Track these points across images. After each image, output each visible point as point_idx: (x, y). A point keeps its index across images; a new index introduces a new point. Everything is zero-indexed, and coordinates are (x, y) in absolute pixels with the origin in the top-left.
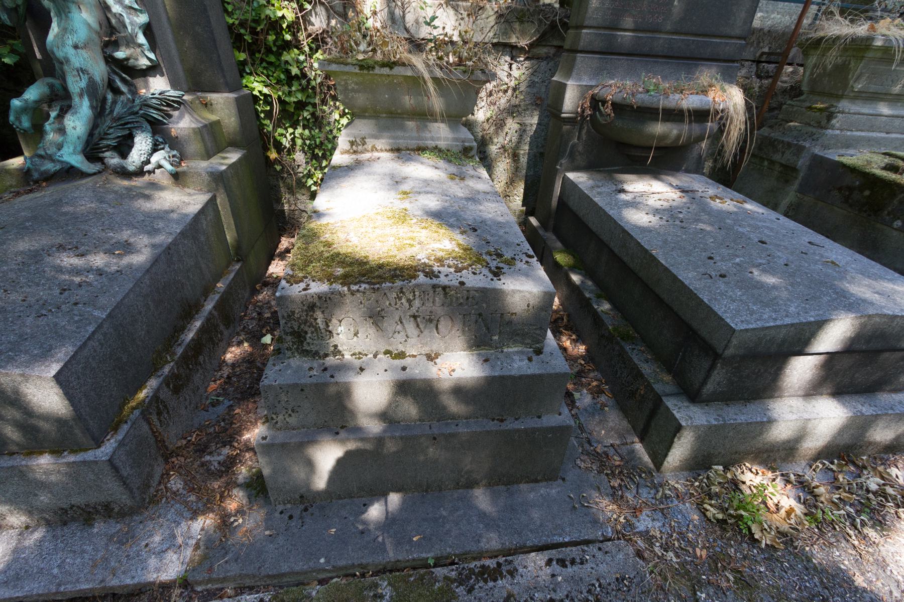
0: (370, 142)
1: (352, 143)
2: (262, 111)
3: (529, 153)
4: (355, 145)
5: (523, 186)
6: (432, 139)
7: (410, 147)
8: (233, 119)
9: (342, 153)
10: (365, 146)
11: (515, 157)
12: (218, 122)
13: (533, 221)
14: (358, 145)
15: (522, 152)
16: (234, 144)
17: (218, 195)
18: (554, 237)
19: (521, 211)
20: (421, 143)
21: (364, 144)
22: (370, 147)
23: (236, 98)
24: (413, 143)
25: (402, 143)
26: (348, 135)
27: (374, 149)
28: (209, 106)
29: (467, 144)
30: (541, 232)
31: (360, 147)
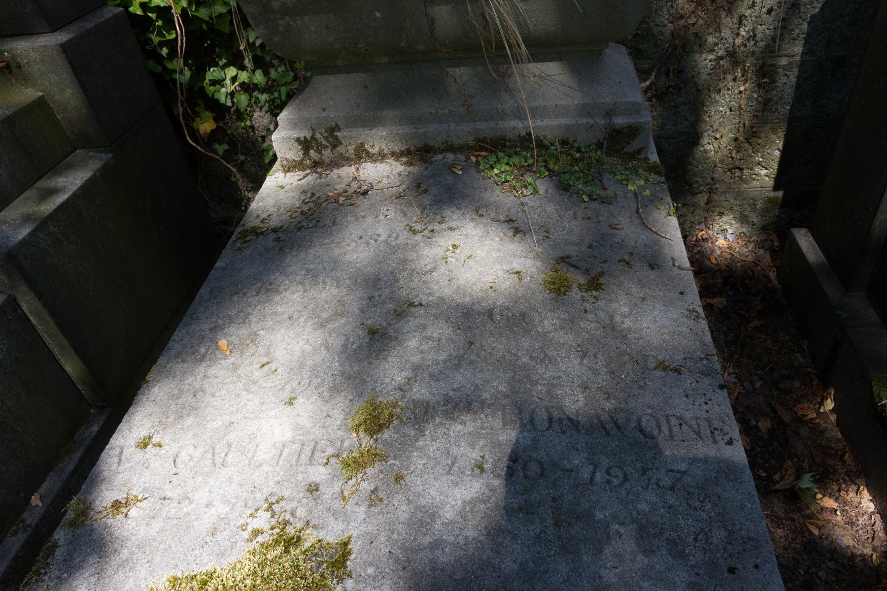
0: (350, 139)
1: (305, 145)
2: (162, 44)
3: (803, 64)
4: (319, 151)
5: (780, 143)
6: (519, 114)
7: (457, 142)
8: (69, 92)
9: (287, 169)
10: (340, 149)
11: (765, 74)
12: (41, 103)
13: (805, 241)
14: (320, 148)
15: (784, 61)
16: (85, 142)
17: (18, 296)
18: (872, 316)
19: (770, 200)
20: (486, 128)
21: (335, 143)
22: (351, 149)
23: (64, 48)
24: (463, 133)
25: (434, 133)
26: (294, 125)
27: (362, 155)
28: (15, 70)
29: (619, 121)
30: (831, 289)
31: (327, 153)
